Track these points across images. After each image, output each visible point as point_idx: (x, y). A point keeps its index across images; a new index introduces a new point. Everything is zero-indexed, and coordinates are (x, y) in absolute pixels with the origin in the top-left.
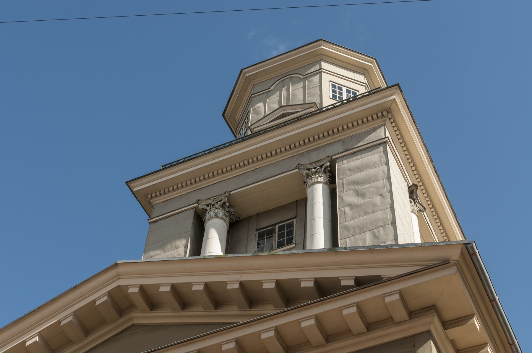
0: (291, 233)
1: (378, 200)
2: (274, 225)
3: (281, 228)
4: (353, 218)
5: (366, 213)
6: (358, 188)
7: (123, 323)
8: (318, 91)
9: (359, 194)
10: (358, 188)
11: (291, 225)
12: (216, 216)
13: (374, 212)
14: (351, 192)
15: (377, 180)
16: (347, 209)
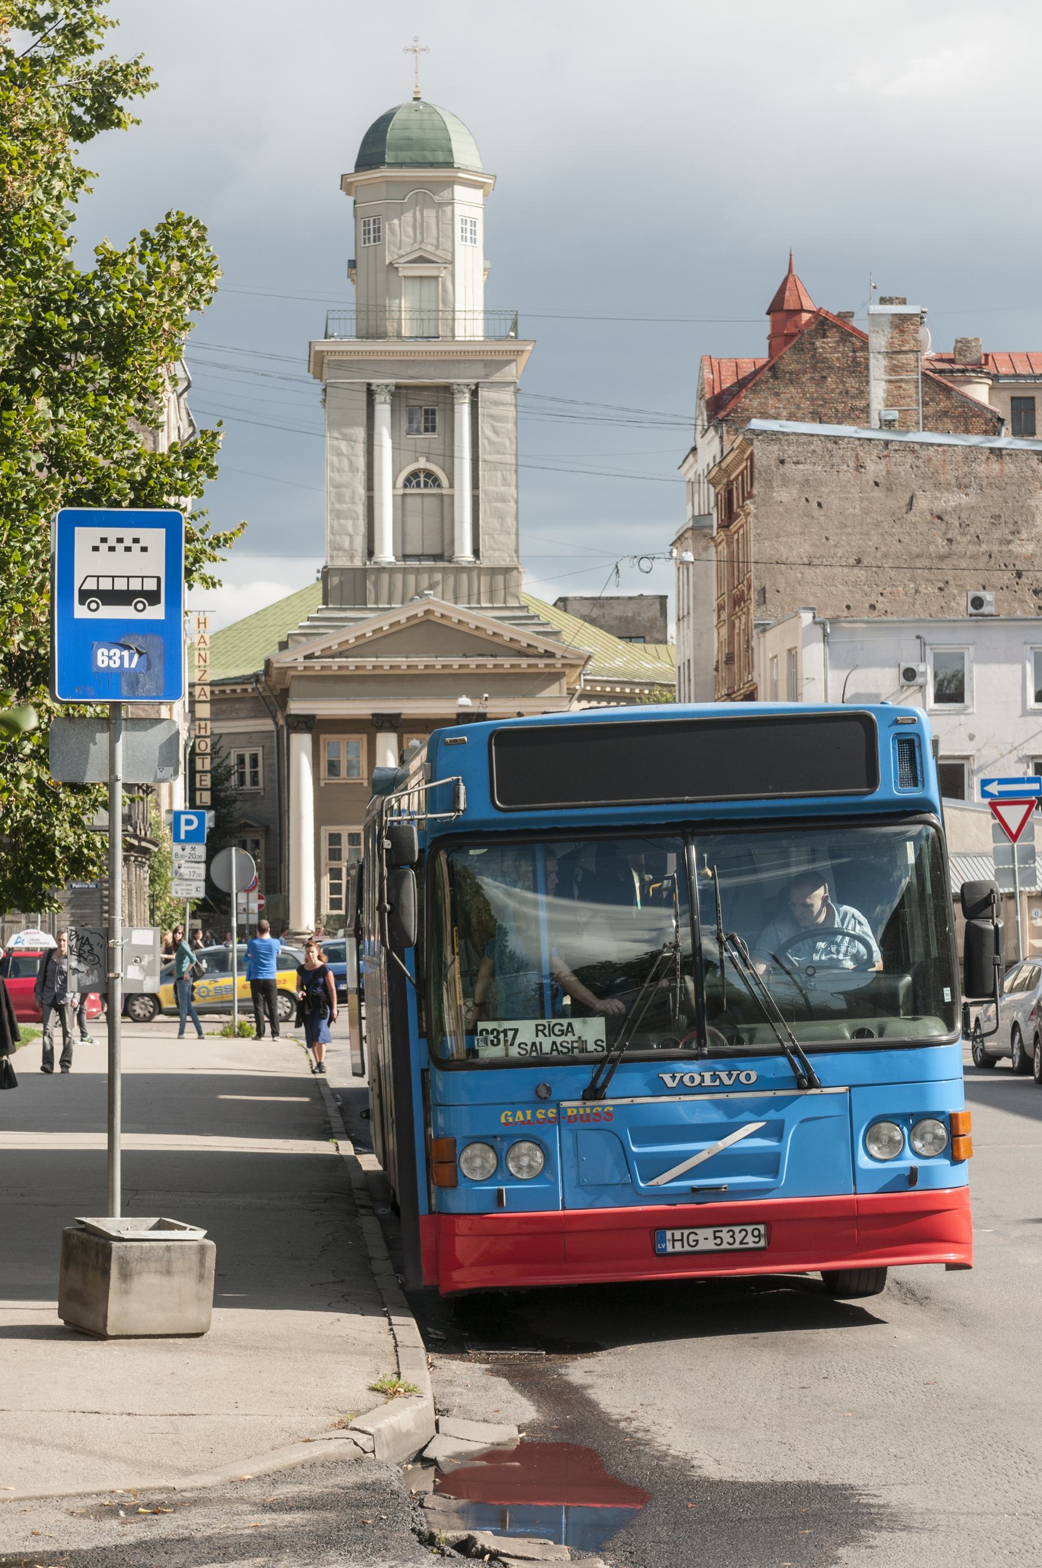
0: (434, 421)
1: (507, 443)
2: (421, 407)
3: (426, 412)
4: (490, 454)
5: (499, 453)
6: (496, 424)
7: (425, 619)
8: (450, 234)
9: (496, 432)
10: (496, 424)
11: (433, 412)
12: (385, 402)
13: (504, 453)
14: (489, 426)
15: (508, 422)
16: (486, 442)
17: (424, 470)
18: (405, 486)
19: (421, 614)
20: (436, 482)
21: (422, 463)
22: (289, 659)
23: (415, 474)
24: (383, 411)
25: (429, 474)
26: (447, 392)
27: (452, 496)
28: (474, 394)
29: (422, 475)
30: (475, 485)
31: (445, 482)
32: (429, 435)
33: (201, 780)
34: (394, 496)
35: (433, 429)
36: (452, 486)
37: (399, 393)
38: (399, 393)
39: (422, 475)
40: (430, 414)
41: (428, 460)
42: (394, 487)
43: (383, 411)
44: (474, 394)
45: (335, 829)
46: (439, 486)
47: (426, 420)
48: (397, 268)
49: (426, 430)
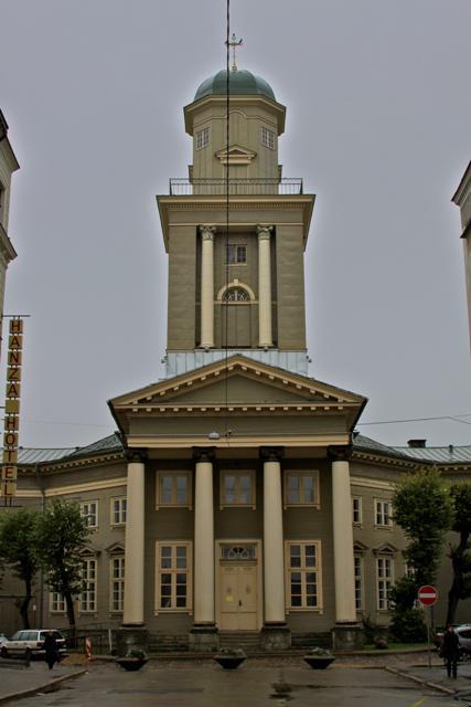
0: (244, 255)
3: (239, 249)
7: (234, 373)
11: (244, 249)
17: (235, 288)
18: (224, 300)
19: (231, 368)
20: (246, 296)
21: (236, 283)
22: (127, 403)
23: (230, 291)
24: (207, 245)
25: (241, 290)
26: (252, 234)
27: (258, 305)
28: (273, 234)
29: (236, 292)
30: (274, 297)
31: (252, 296)
32: (241, 264)
33: (7, 472)
34: (215, 306)
35: (244, 260)
36: (257, 298)
37: (219, 235)
38: (219, 235)
39: (236, 292)
40: (241, 250)
41: (240, 280)
42: (215, 298)
43: (207, 245)
44: (273, 234)
45: (166, 543)
46: (249, 299)
47: (239, 254)
48: (219, 158)
49: (239, 261)
